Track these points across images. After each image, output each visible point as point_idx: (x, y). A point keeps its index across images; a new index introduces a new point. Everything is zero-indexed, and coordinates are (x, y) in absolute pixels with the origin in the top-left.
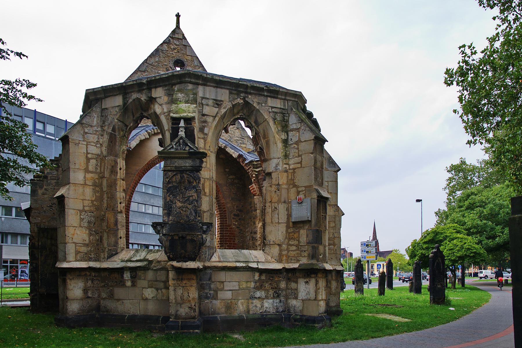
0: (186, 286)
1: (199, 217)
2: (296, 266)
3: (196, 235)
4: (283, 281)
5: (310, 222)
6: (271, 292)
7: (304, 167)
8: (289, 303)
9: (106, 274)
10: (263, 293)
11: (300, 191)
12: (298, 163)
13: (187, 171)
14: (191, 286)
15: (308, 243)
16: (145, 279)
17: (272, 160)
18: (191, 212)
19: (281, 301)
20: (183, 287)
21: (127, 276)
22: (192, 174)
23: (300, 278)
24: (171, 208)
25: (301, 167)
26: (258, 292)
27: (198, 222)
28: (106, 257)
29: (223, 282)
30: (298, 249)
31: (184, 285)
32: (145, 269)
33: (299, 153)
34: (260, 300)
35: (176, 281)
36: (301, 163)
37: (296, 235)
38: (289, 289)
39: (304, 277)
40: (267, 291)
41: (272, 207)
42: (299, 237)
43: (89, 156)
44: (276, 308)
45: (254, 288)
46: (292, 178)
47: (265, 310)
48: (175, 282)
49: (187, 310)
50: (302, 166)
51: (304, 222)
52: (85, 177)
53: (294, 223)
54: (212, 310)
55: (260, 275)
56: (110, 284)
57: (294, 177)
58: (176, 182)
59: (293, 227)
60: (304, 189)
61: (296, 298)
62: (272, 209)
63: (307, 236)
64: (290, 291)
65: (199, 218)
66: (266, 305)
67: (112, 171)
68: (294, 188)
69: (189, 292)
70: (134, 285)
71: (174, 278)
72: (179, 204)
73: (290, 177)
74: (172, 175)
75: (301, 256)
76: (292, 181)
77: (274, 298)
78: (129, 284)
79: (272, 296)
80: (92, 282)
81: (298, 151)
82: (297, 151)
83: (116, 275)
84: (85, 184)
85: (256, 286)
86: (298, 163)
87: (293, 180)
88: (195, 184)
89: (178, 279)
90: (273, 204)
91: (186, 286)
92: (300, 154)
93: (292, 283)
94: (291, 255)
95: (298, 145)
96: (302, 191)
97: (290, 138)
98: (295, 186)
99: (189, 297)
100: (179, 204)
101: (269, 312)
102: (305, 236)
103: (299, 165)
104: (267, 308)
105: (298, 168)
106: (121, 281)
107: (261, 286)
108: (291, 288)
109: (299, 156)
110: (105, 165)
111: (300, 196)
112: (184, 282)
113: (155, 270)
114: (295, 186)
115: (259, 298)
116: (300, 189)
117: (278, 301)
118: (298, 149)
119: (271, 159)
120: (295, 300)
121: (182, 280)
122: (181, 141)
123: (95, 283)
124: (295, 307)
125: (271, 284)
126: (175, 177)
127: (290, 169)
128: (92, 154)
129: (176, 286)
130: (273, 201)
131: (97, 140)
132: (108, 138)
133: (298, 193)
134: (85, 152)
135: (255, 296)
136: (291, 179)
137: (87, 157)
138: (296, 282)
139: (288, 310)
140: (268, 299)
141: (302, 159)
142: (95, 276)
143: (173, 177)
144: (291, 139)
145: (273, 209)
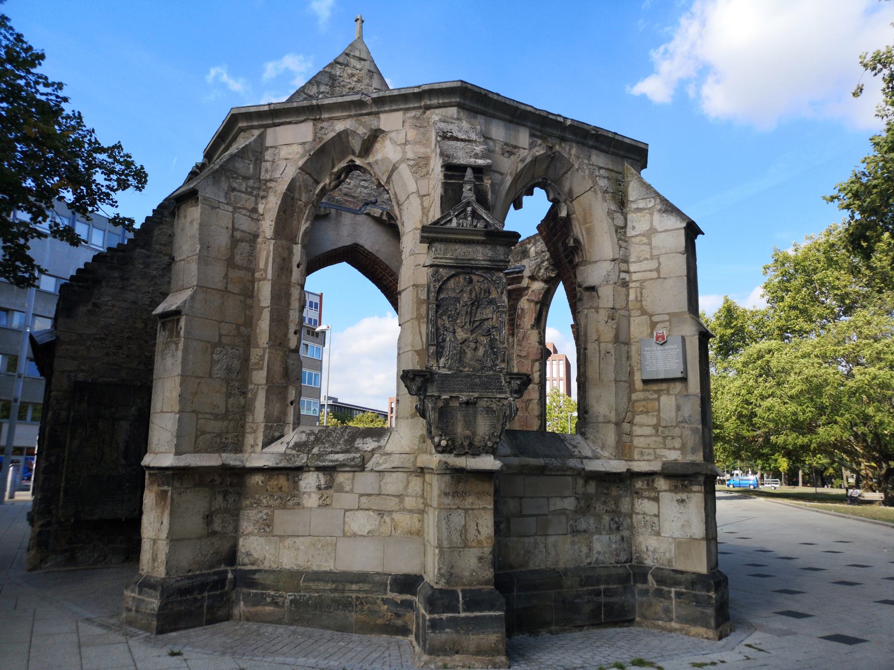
0: (473, 509)
1: (503, 361)
2: (656, 466)
3: (495, 398)
4: (625, 497)
6: (606, 519)
7: (664, 278)
8: (640, 543)
10: (592, 521)
11: (657, 323)
13: (478, 268)
17: (598, 264)
18: (486, 351)
19: (623, 538)
20: (466, 510)
22: (488, 276)
24: (444, 340)
25: (659, 278)
26: (582, 519)
27: (500, 372)
29: (521, 498)
30: (657, 435)
31: (468, 507)
33: (651, 252)
34: (586, 536)
35: (450, 498)
36: (658, 270)
38: (637, 514)
39: (674, 489)
40: (599, 517)
41: (600, 351)
43: (238, 235)
44: (615, 553)
45: (576, 512)
46: (636, 297)
47: (597, 559)
48: (448, 501)
50: (661, 276)
52: (226, 276)
53: (646, 382)
54: (500, 559)
55: (586, 482)
56: (264, 501)
57: (641, 296)
58: (454, 290)
59: (644, 390)
60: (667, 318)
62: (600, 354)
64: (640, 517)
65: (503, 365)
66: (597, 546)
67: (282, 269)
68: (644, 317)
69: (480, 521)
71: (447, 491)
72: (461, 335)
74: (448, 276)
75: (665, 448)
76: (639, 304)
77: (610, 531)
79: (607, 528)
80: (224, 497)
81: (651, 248)
84: (226, 290)
85: (579, 506)
86: (651, 271)
87: (641, 301)
89: (455, 494)
90: (602, 344)
91: (473, 509)
92: (655, 253)
93: (646, 501)
94: (641, 445)
95: (650, 238)
96: (663, 322)
99: (479, 532)
101: (603, 563)
103: (654, 275)
104: (599, 553)
105: (651, 279)
107: (588, 507)
108: (644, 514)
109: (652, 257)
111: (661, 332)
112: (470, 500)
115: (585, 531)
116: (656, 319)
117: (615, 537)
118: (650, 244)
119: (596, 262)
120: (655, 538)
121: (463, 495)
123: (231, 500)
124: (654, 551)
125: (605, 502)
126: (452, 281)
128: (243, 231)
129: (450, 509)
130: (602, 339)
131: (253, 205)
132: (279, 202)
133: (653, 325)
134: (230, 226)
135: (578, 528)
137: (232, 236)
139: (637, 558)
140: (601, 534)
141: (659, 264)
142: (231, 485)
143: (449, 279)
144: (634, 228)
145: (602, 355)
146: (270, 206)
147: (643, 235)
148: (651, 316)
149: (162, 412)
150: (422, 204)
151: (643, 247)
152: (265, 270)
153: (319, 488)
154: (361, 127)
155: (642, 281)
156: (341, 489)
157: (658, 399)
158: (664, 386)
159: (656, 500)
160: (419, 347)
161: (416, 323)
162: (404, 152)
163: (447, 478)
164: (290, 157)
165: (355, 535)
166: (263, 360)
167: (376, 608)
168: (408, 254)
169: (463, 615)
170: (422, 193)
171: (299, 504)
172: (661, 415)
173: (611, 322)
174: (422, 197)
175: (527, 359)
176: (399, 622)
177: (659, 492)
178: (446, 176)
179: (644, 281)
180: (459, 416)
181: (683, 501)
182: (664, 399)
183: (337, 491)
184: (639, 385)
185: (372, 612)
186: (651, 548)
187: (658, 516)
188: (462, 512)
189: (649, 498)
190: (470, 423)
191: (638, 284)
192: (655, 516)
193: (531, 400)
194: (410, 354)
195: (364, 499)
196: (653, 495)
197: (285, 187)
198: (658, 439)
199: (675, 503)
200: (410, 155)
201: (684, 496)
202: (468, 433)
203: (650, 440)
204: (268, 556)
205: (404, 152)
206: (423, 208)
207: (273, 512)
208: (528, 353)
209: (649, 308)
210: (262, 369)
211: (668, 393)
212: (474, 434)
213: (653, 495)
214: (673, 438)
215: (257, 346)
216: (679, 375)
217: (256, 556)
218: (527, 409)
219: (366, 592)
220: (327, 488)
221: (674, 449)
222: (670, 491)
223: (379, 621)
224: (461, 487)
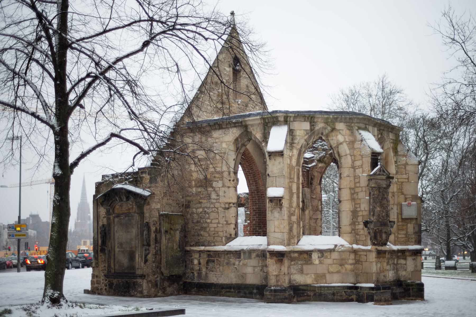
5: (416, 219)
9: (296, 255)
11: (407, 198)
12: (406, 179)
14: (384, 262)
15: (415, 233)
16: (330, 258)
20: (380, 262)
21: (315, 256)
23: (409, 256)
24: (374, 211)
25: (408, 182)
28: (296, 243)
32: (331, 251)
36: (408, 179)
37: (404, 227)
42: (407, 229)
49: (383, 277)
51: (411, 219)
53: (402, 219)
57: (402, 188)
61: (406, 270)
63: (414, 228)
68: (403, 195)
70: (321, 263)
73: (399, 188)
78: (317, 262)
81: (406, 170)
82: (404, 170)
83: (305, 256)
86: (406, 179)
87: (402, 190)
88: (386, 196)
97: (398, 160)
98: (403, 193)
100: (378, 209)
102: (412, 228)
103: (407, 180)
106: (310, 260)
109: (406, 174)
110: (294, 173)
112: (381, 259)
113: (339, 252)
114: (403, 193)
122: (382, 169)
124: (404, 276)
127: (398, 182)
132: (298, 152)
136: (400, 189)
138: (405, 259)
141: (409, 177)
146: (294, 153)
147: (402, 165)
148: (405, 195)
149: (275, 232)
150: (351, 158)
151: (402, 170)
152: (294, 178)
153: (319, 257)
154: (329, 127)
155: (402, 182)
156: (326, 258)
157: (407, 225)
158: (409, 221)
159: (405, 259)
160: (352, 210)
161: (351, 201)
162: (345, 139)
163: (376, 253)
164: (300, 135)
165: (332, 273)
166: (295, 212)
167: (342, 294)
168: (345, 176)
169: (382, 291)
170: (351, 154)
171: (312, 263)
172: (408, 230)
173: (393, 197)
174: (351, 156)
175: (316, 200)
176: (350, 298)
177: (406, 256)
178: (372, 156)
179: (403, 182)
180: (378, 234)
181: (414, 259)
182: (409, 225)
183: (325, 258)
184: (400, 220)
185: (341, 296)
186: (403, 275)
187: (406, 264)
188: (379, 263)
189: (403, 259)
190: (381, 236)
191: (400, 183)
192: (405, 264)
193: (317, 219)
194: (349, 212)
195: (335, 261)
196: (404, 257)
197: (300, 147)
198: (406, 238)
199: (412, 260)
200: (347, 140)
201: (415, 257)
202: (381, 239)
203: (403, 239)
204: (302, 281)
205: (345, 139)
206: (352, 160)
207: (302, 266)
208: (316, 196)
209: (405, 193)
210: (295, 215)
211: (411, 223)
212: (382, 239)
213: (404, 257)
214: (412, 238)
215: (293, 207)
216: (415, 217)
217: (297, 281)
218: (316, 222)
219: (339, 290)
220: (321, 257)
221: (412, 242)
222: (410, 256)
223: (344, 298)
224: (379, 256)
